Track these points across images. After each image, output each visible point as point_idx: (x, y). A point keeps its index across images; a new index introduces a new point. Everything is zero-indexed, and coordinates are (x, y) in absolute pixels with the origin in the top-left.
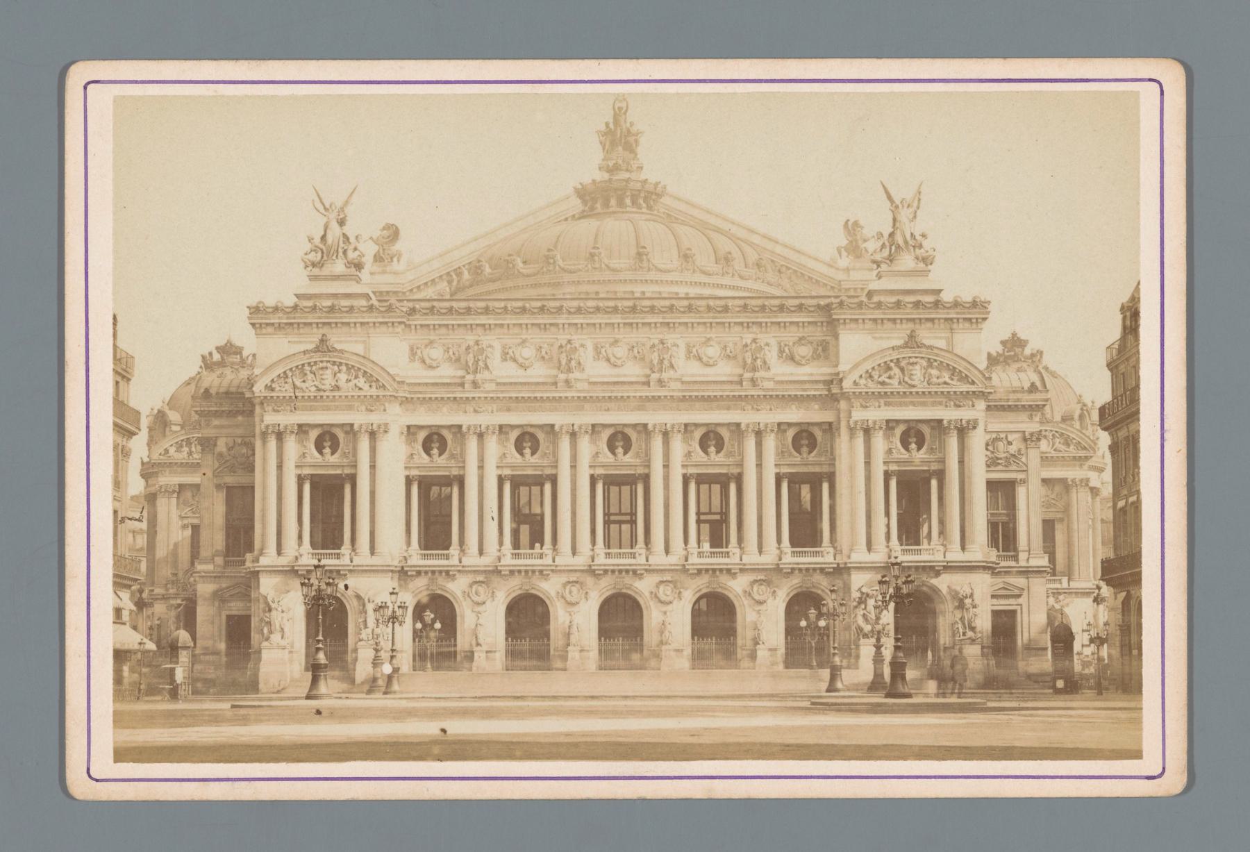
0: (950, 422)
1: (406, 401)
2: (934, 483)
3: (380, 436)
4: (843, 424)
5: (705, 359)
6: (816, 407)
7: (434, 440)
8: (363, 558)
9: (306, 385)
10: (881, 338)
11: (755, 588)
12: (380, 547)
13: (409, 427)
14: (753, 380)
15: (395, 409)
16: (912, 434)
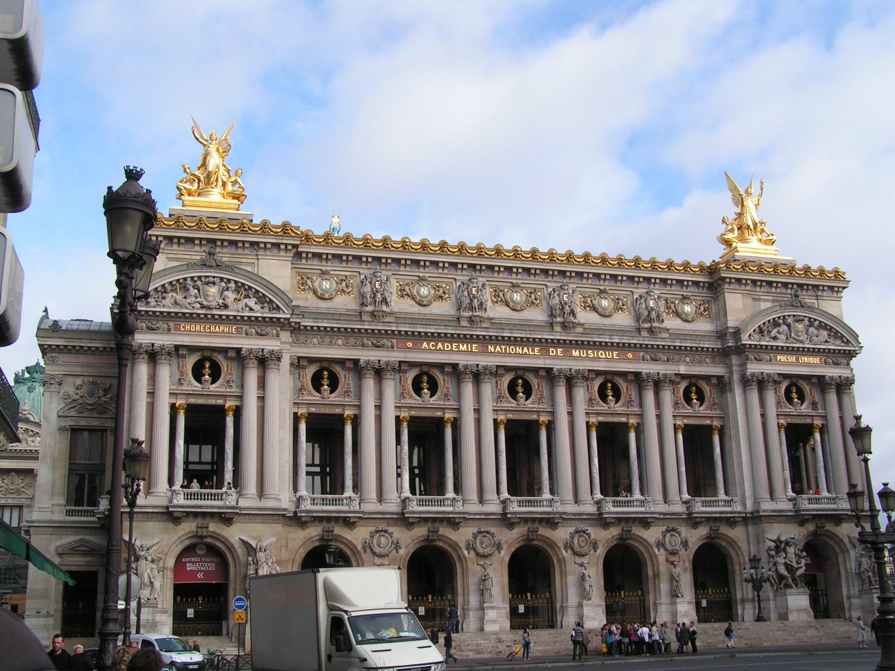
0: (832, 378)
1: (296, 330)
2: (817, 436)
3: (271, 364)
4: (736, 377)
5: (600, 310)
6: (708, 360)
7: (325, 375)
8: (249, 501)
9: (189, 300)
10: (759, 300)
11: (667, 539)
12: (268, 491)
13: (299, 358)
14: (651, 330)
15: (285, 336)
16: (795, 388)
